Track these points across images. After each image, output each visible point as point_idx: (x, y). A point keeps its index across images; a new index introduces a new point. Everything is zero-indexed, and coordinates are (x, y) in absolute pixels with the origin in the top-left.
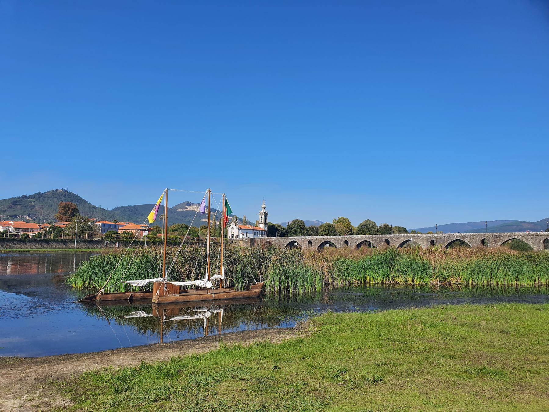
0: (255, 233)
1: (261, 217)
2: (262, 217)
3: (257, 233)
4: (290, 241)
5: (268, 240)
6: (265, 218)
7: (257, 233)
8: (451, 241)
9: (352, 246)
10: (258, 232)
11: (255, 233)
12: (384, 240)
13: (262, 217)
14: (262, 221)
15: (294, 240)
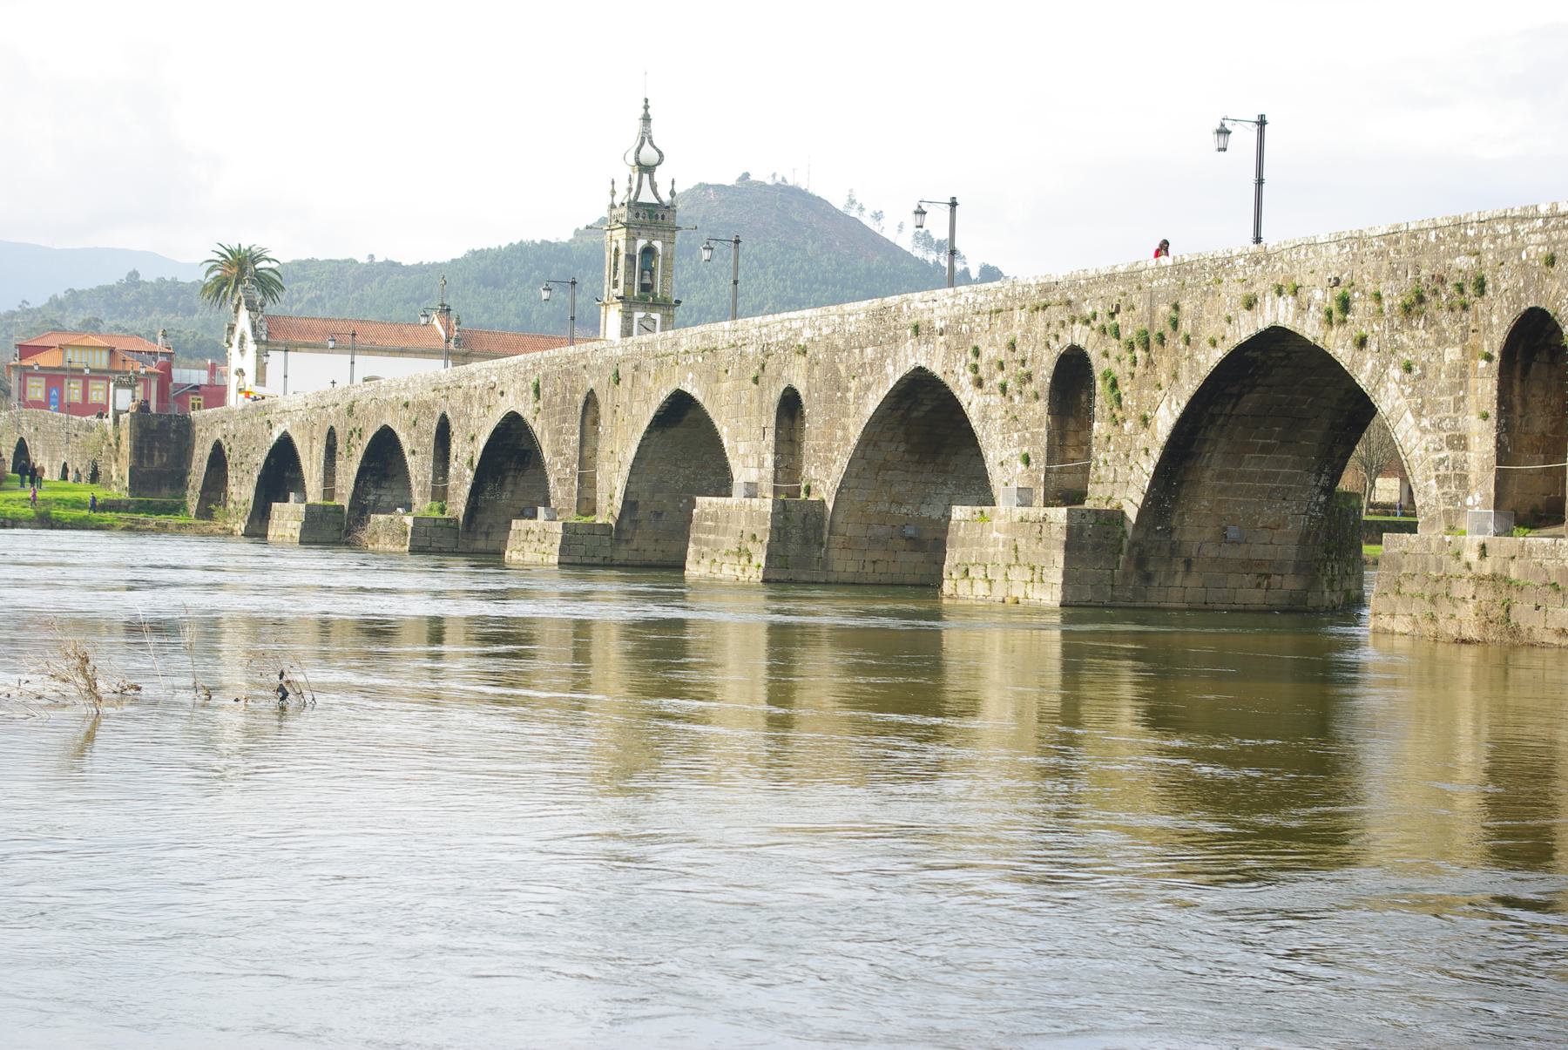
6: (649, 251)
14: (616, 285)
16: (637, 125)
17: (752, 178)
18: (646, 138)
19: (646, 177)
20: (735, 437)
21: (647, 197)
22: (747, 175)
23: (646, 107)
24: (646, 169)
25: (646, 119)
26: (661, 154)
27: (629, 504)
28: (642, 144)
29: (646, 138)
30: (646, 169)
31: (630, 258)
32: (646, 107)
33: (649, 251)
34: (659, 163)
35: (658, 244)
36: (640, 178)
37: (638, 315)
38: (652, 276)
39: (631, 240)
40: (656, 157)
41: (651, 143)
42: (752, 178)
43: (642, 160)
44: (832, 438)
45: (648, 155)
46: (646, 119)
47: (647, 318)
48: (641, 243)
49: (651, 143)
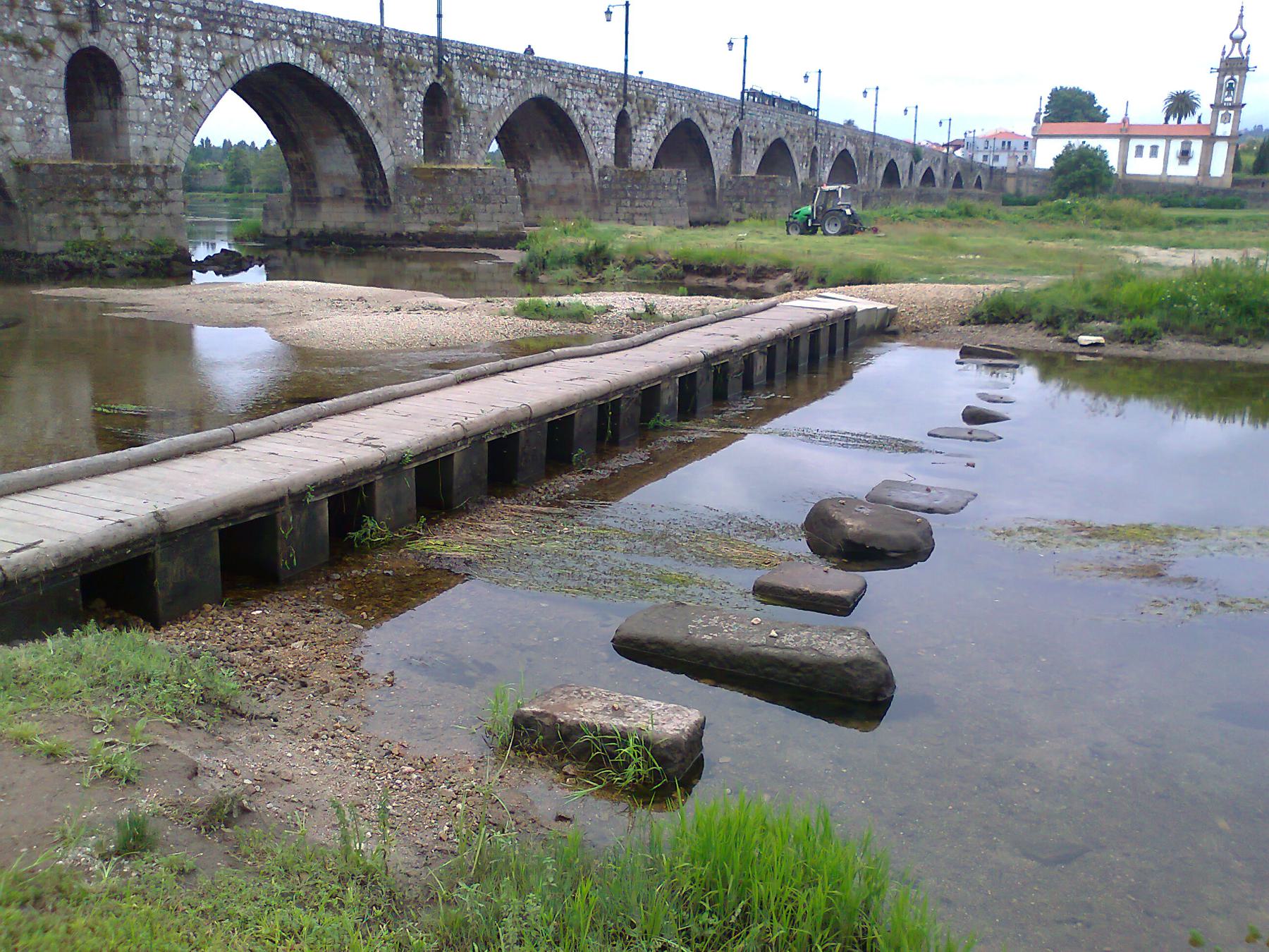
0: (1140, 149)
10: (1161, 143)
11: (1140, 149)
18: (1240, 24)
19: (1237, 45)
21: (1236, 54)
23: (1242, 11)
24: (1237, 41)
25: (1241, 17)
26: (1245, 33)
28: (1237, 28)
29: (1240, 24)
30: (1237, 41)
32: (1242, 11)
34: (1244, 37)
35: (1237, 77)
36: (1234, 45)
37: (1222, 112)
41: (1242, 28)
45: (1239, 33)
46: (1241, 17)
47: (1227, 113)
49: (1242, 28)
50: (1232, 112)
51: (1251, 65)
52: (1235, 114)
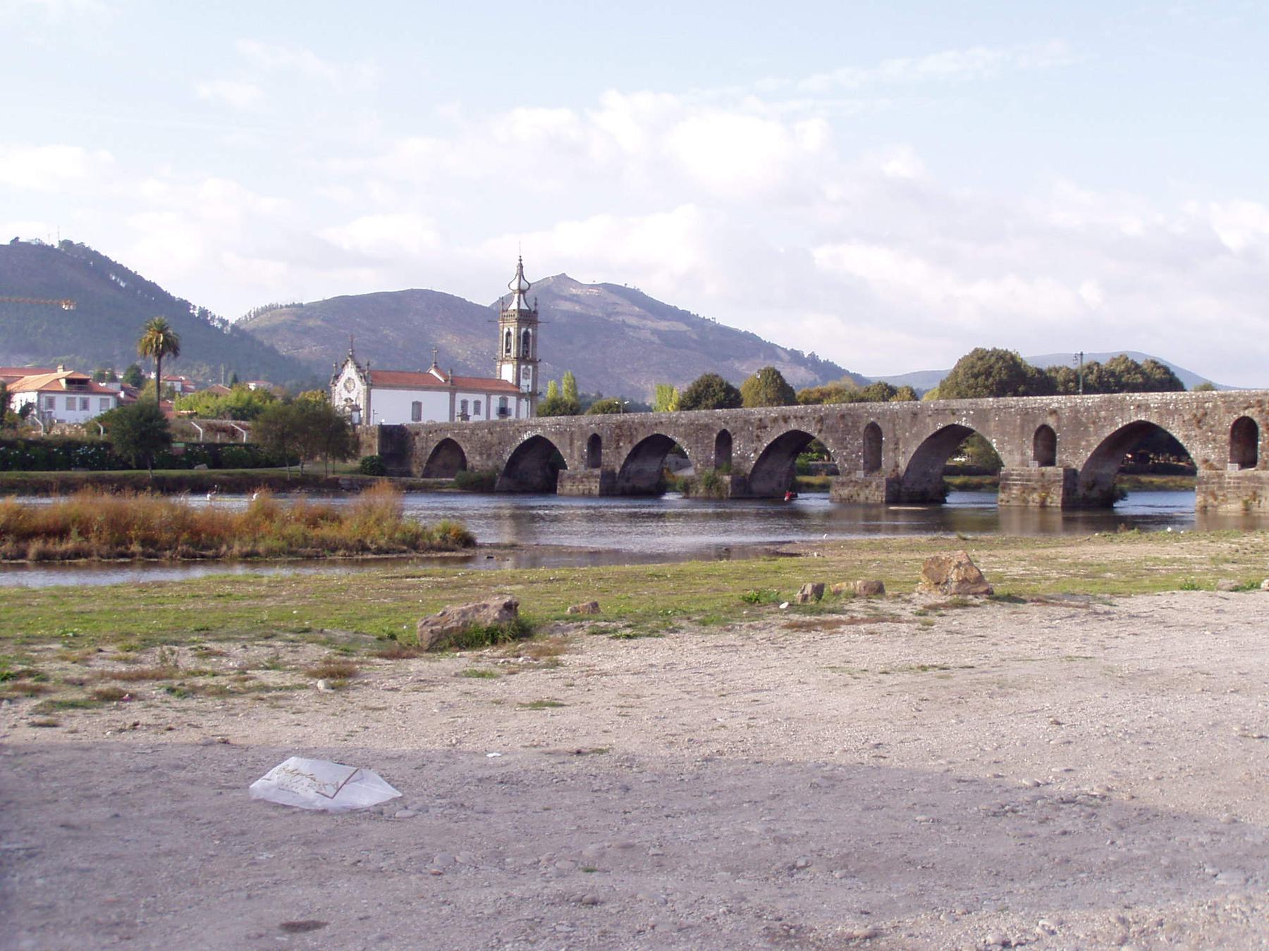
0: (465, 403)
1: (506, 330)
2: (509, 334)
3: (477, 403)
4: (526, 437)
5: (449, 436)
6: (526, 333)
7: (477, 403)
8: (1114, 429)
9: (745, 458)
10: (482, 398)
11: (465, 403)
12: (862, 430)
13: (509, 334)
14: (508, 351)
15: (539, 432)
16: (515, 270)
17: (20, 240)
20: (1000, 442)
22: (17, 238)
23: (521, 260)
27: (908, 469)
31: (519, 337)
32: (521, 260)
33: (526, 333)
37: (523, 367)
38: (528, 347)
39: (519, 328)
40: (528, 286)
42: (20, 240)
43: (522, 288)
44: (1079, 445)
46: (521, 266)
47: (526, 368)
48: (523, 330)
50: (530, 367)
51: (539, 319)
52: (533, 370)
